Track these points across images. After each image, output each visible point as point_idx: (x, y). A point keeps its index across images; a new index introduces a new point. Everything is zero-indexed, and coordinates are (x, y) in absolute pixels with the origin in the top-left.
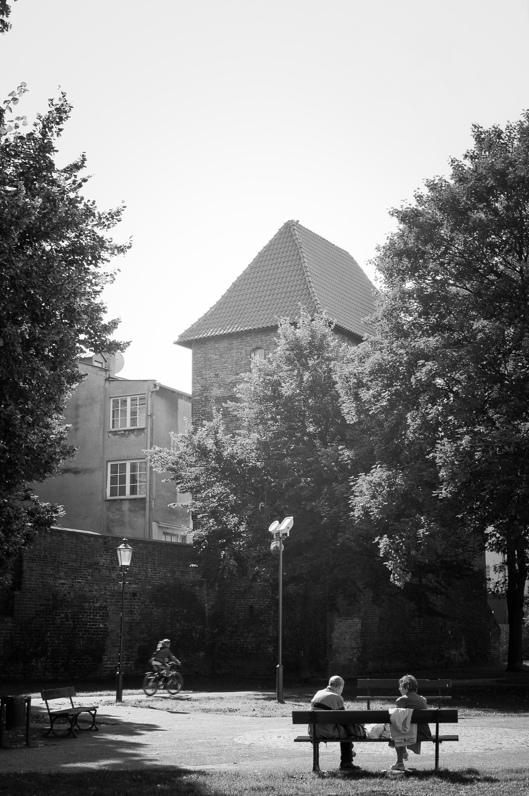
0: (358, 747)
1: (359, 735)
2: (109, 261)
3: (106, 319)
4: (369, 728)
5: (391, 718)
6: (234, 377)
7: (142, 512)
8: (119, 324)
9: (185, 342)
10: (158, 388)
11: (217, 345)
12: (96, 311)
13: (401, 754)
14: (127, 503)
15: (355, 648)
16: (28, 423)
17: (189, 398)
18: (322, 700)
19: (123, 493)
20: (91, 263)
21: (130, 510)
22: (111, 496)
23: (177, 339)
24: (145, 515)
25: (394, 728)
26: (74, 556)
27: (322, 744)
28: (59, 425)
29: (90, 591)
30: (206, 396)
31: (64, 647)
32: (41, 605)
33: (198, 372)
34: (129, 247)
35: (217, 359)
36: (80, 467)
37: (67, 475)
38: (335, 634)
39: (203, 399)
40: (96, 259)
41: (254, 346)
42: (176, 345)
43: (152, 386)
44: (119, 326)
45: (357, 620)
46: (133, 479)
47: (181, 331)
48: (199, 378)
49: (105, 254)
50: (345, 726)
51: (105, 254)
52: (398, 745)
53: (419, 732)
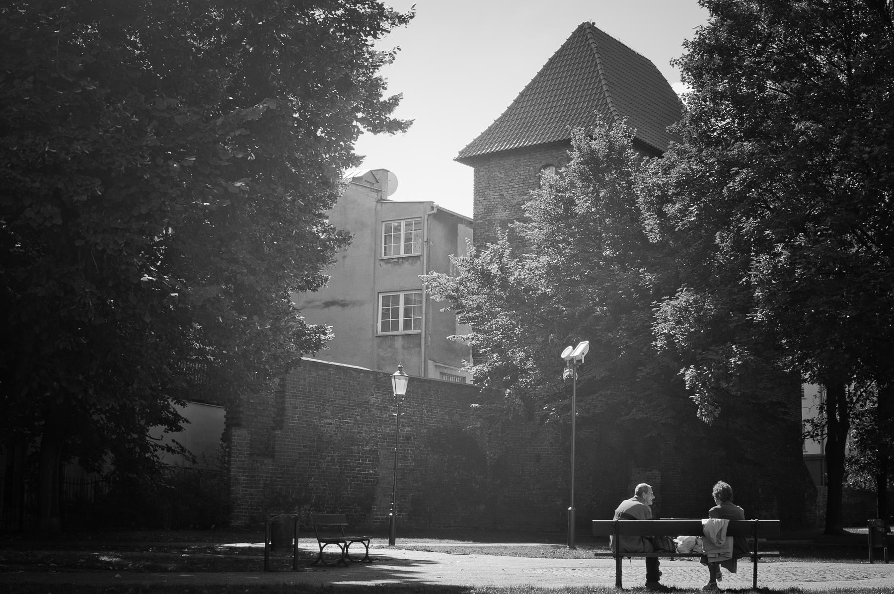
0: (665, 564)
1: (667, 549)
2: (389, 32)
3: (385, 96)
4: (680, 540)
5: (705, 529)
7: (417, 350)
8: (401, 101)
9: (465, 158)
10: (435, 211)
11: (502, 162)
12: (375, 86)
13: (715, 575)
14: (400, 338)
16: (300, 210)
17: (469, 223)
18: (628, 510)
20: (369, 34)
21: (404, 347)
22: (382, 331)
23: (457, 155)
24: (420, 352)
25: (708, 541)
26: (342, 394)
27: (625, 562)
28: (332, 217)
29: (359, 433)
33: (479, 192)
34: (412, 17)
36: (348, 298)
37: (334, 309)
40: (376, 30)
41: (544, 163)
43: (429, 208)
44: (401, 102)
46: (407, 312)
47: (462, 147)
49: (385, 25)
50: (650, 540)
51: (385, 25)
52: (710, 561)
53: (735, 546)
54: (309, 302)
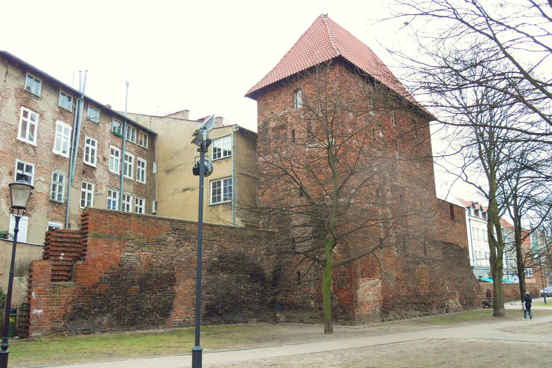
9: (254, 95)
15: (377, 302)
19: (219, 200)
21: (223, 210)
22: (213, 202)
23: (246, 93)
26: (142, 234)
31: (130, 306)
32: (105, 273)
33: (260, 113)
38: (360, 291)
42: (248, 98)
45: (377, 280)
54: (176, 190)
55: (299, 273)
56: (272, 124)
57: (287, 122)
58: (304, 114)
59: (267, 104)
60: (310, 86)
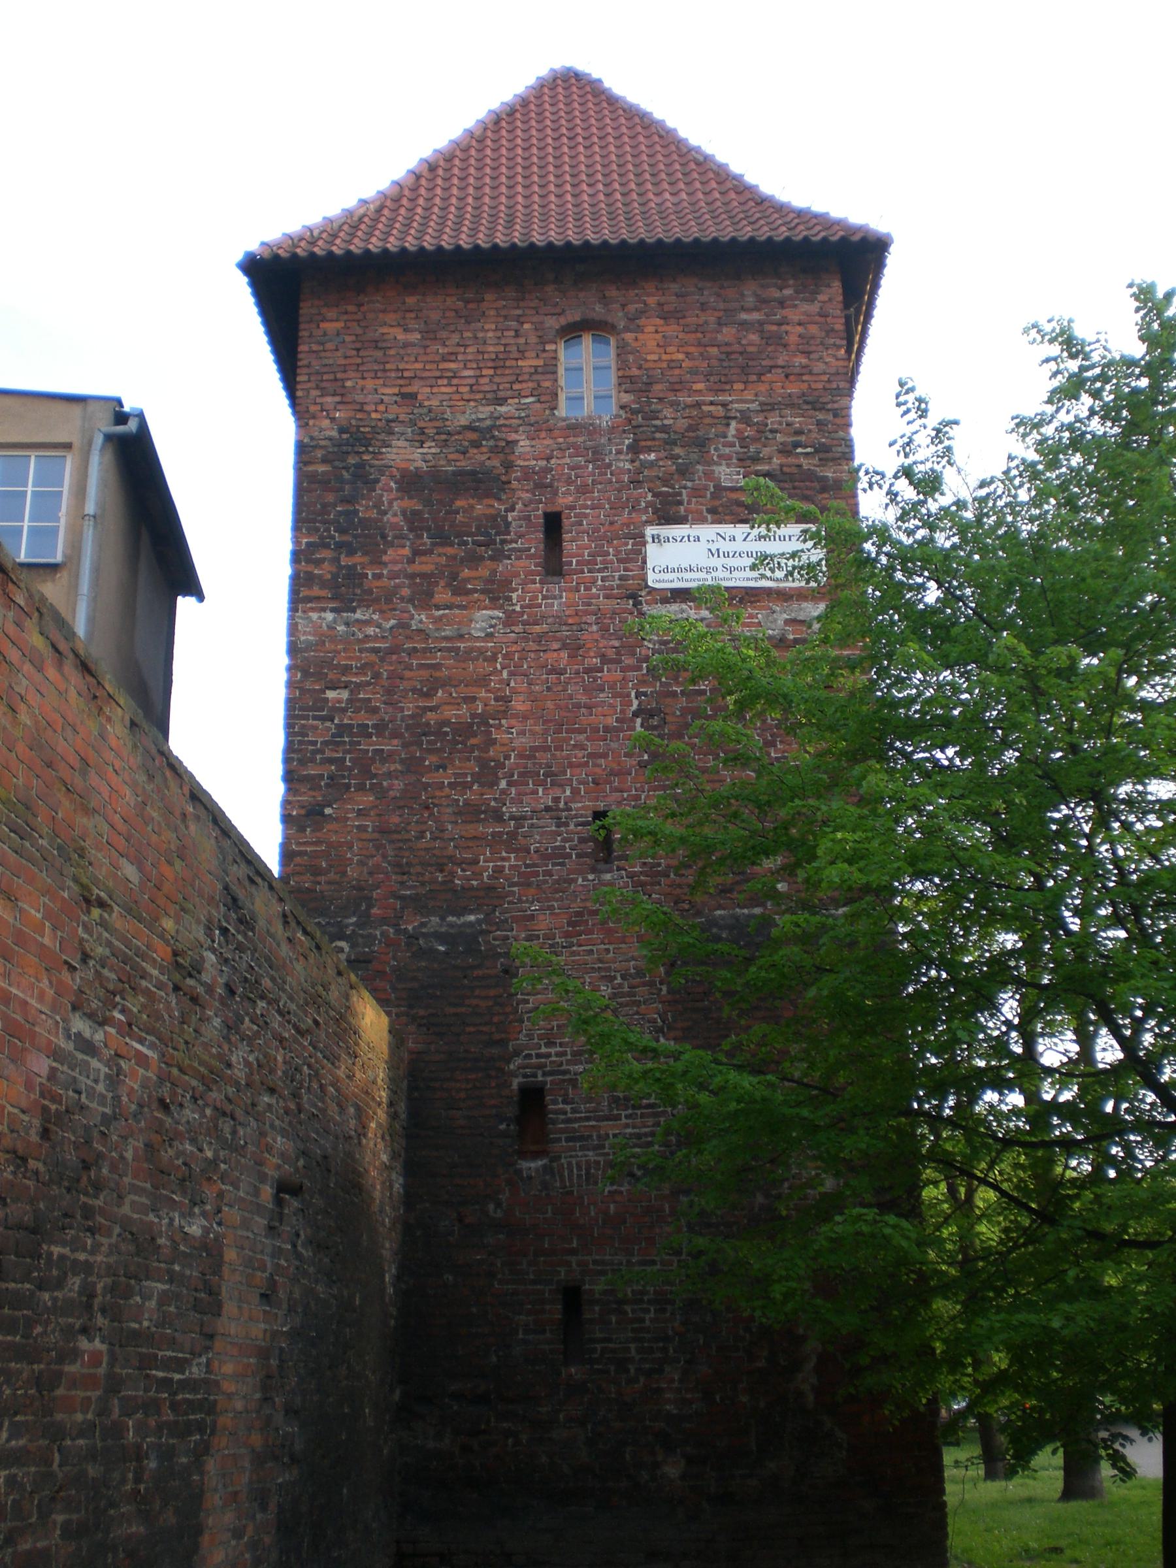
6: (485, 411)
30: (357, 466)
35: (406, 345)
39: (346, 475)
41: (574, 316)
43: (109, 416)
48: (329, 399)
55: (572, 1297)
56: (404, 454)
57: (508, 466)
58: (635, 449)
59: (376, 344)
60: (672, 330)
